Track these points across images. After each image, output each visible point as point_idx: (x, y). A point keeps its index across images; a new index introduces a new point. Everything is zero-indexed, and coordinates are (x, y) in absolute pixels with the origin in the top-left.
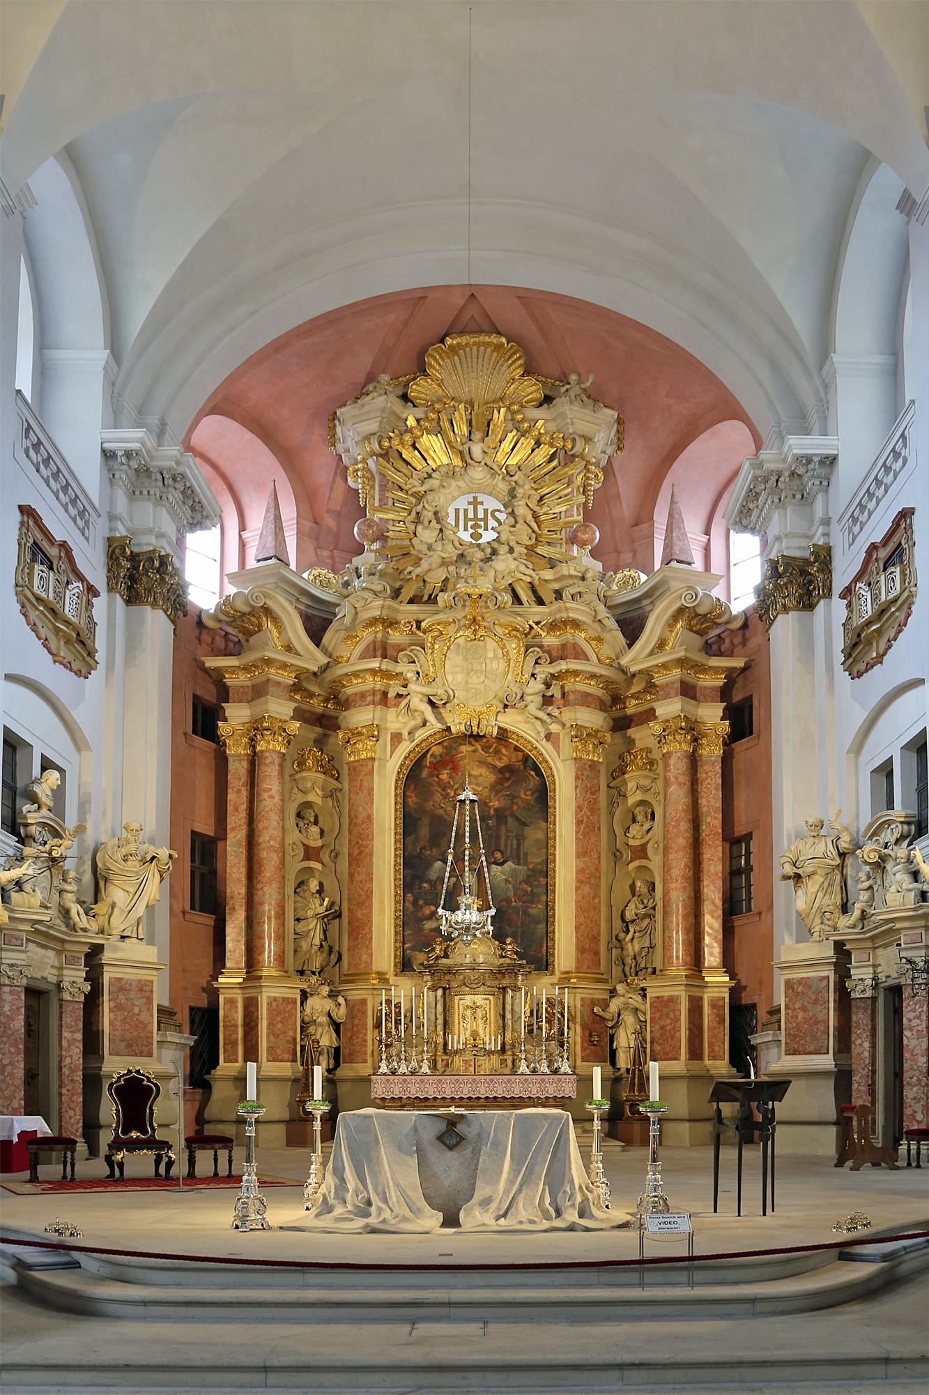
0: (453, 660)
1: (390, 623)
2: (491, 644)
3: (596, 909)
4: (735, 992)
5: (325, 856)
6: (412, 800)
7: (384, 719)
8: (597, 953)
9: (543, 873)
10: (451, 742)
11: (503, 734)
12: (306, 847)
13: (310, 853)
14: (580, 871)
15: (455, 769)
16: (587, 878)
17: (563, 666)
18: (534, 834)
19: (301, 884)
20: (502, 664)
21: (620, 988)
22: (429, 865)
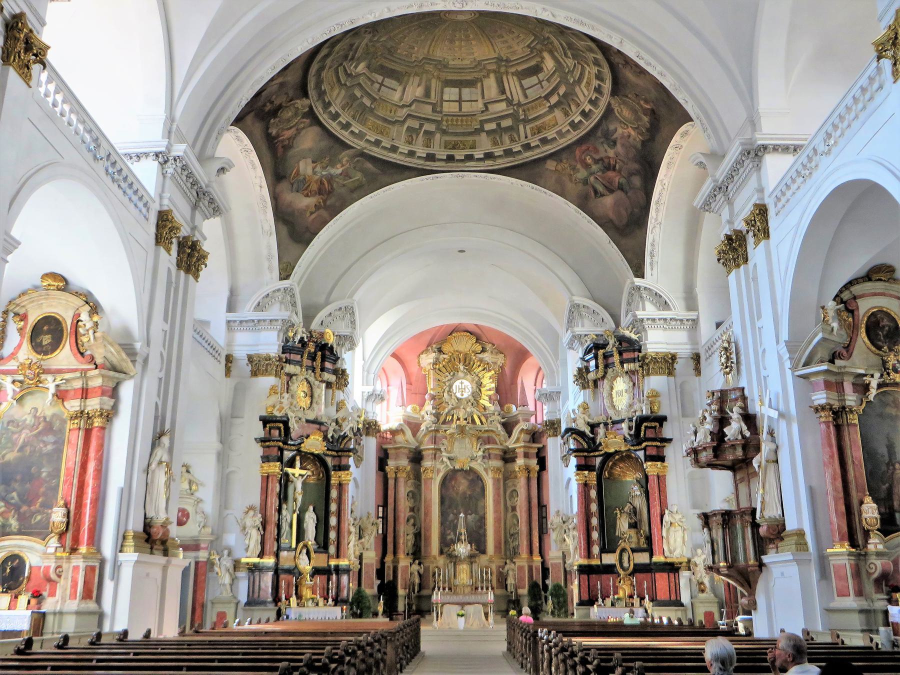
0: (456, 444)
1: (437, 431)
2: (467, 440)
3: (500, 532)
4: (543, 563)
5: (416, 511)
6: (443, 491)
7: (435, 464)
8: (501, 548)
9: (482, 520)
10: (455, 471)
11: (471, 469)
12: (410, 508)
13: (412, 509)
14: (495, 518)
15: (456, 480)
16: (497, 520)
17: (487, 447)
18: (480, 504)
19: (408, 521)
20: (471, 446)
21: (508, 561)
22: (449, 515)
